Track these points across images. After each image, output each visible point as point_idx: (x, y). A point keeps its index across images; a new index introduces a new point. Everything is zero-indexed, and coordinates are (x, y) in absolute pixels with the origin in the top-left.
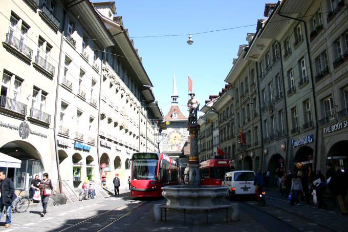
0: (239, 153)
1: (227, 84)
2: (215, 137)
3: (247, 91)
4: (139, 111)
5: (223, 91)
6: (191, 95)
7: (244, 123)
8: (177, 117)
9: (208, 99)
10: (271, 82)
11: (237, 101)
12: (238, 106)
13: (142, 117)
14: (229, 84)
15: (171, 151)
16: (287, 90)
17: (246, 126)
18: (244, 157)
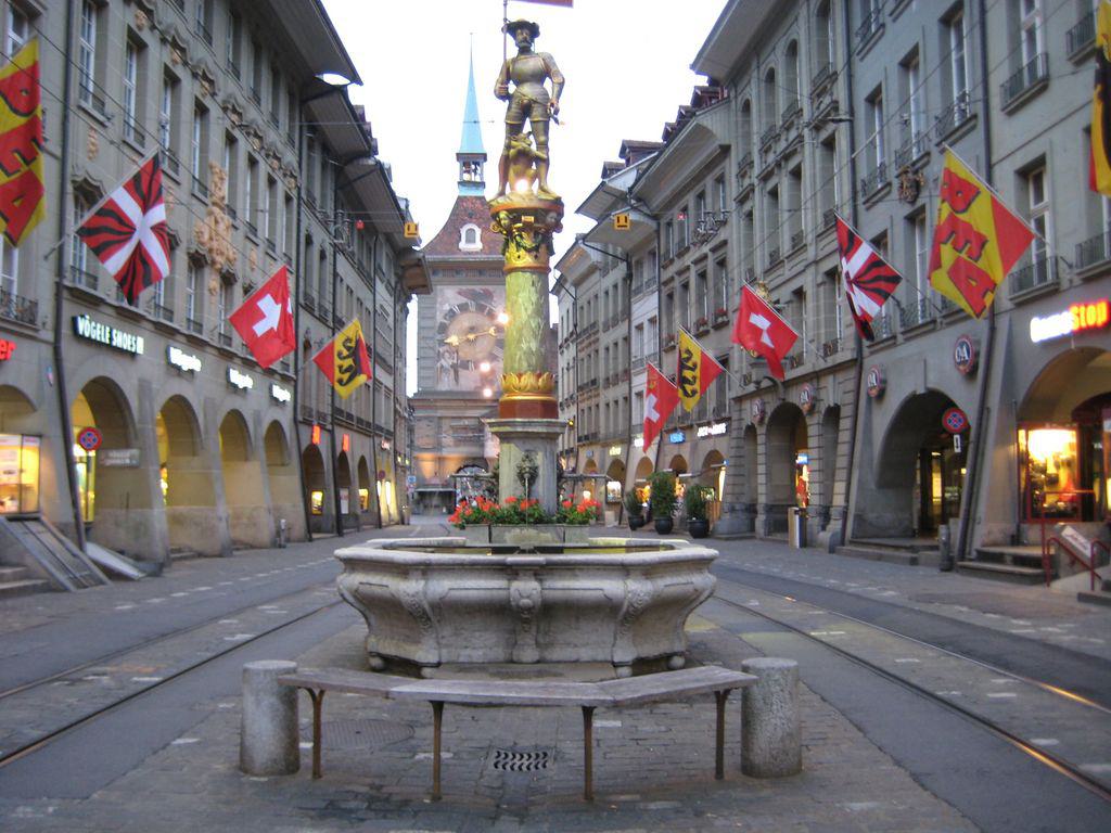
0: (750, 396)
1: (703, 81)
2: (640, 328)
3: (794, 111)
4: (294, 194)
5: (685, 116)
6: (513, 28)
7: (775, 262)
8: (478, 245)
9: (616, 159)
10: (914, 52)
11: (745, 166)
12: (747, 182)
13: (309, 223)
14: (713, 82)
15: (455, 388)
16: (1000, 76)
17: (786, 271)
18: (769, 410)
